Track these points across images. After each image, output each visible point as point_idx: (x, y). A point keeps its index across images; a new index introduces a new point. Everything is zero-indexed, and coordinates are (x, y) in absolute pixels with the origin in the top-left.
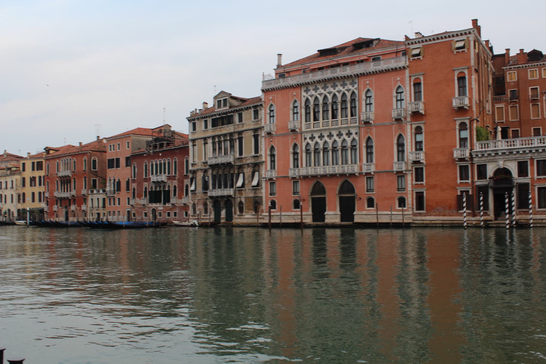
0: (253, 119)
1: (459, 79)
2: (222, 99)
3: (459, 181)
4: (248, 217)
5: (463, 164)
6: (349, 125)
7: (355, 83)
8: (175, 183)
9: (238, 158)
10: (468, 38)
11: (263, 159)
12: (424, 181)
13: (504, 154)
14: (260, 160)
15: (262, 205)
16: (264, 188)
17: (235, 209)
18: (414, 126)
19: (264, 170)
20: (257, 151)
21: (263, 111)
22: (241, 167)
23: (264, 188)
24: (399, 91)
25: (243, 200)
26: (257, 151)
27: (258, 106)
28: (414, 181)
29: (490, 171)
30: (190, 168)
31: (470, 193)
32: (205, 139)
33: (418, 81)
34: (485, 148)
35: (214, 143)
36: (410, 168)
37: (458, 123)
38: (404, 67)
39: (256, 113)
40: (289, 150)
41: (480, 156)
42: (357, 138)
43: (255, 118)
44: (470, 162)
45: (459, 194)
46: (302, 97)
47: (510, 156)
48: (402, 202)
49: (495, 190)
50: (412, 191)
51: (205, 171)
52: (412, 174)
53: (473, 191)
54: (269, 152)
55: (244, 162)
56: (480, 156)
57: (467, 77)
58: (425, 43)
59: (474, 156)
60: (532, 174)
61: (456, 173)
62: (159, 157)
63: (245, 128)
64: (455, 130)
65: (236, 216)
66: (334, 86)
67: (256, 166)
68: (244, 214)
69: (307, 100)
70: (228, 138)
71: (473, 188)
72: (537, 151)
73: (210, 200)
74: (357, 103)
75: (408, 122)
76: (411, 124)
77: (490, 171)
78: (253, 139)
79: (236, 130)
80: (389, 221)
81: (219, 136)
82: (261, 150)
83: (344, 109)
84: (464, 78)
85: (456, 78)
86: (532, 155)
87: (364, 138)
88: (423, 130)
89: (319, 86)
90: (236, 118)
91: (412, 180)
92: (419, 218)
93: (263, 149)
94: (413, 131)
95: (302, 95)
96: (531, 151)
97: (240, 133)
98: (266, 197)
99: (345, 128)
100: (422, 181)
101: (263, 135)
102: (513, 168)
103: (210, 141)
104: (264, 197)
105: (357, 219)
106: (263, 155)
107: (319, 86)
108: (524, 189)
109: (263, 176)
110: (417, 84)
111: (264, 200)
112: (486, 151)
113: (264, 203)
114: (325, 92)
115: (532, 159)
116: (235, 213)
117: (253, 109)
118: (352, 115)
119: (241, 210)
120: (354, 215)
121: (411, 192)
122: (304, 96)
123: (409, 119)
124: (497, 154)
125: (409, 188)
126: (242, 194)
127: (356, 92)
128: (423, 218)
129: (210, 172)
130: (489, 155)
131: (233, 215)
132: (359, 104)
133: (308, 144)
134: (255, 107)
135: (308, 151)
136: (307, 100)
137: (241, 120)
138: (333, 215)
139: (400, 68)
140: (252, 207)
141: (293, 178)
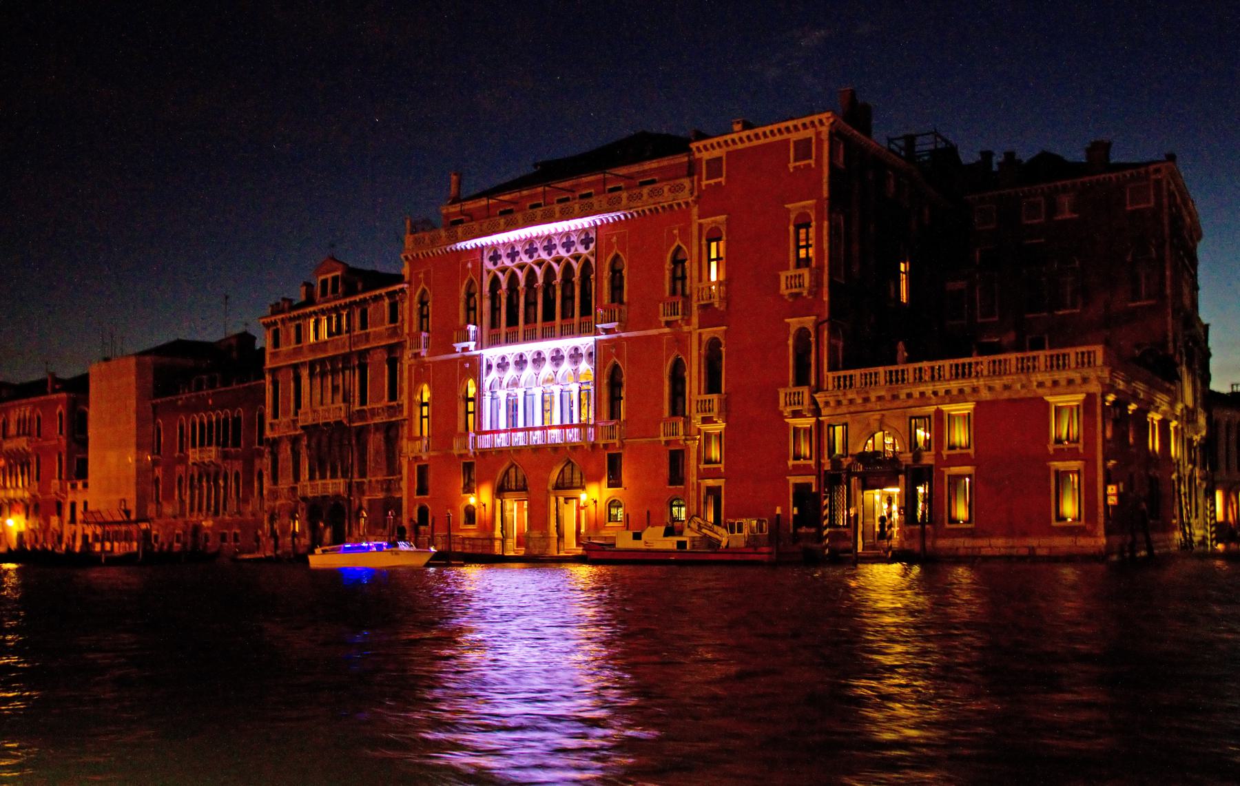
1: (798, 228)
8: (238, 466)
10: (818, 134)
20: (393, 395)
21: (406, 304)
24: (680, 257)
26: (393, 395)
30: (269, 434)
31: (814, 490)
32: (296, 367)
35: (312, 375)
39: (394, 308)
41: (832, 404)
47: (896, 404)
51: (295, 440)
53: (818, 486)
56: (832, 404)
58: (732, 148)
59: (821, 405)
62: (206, 409)
64: (787, 346)
71: (818, 478)
73: (303, 505)
81: (322, 362)
82: (401, 393)
83: (567, 299)
97: (363, 354)
103: (305, 373)
114: (530, 261)
117: (387, 301)
122: (489, 272)
125: (693, 479)
127: (592, 260)
129: (304, 442)
141: (461, 456)
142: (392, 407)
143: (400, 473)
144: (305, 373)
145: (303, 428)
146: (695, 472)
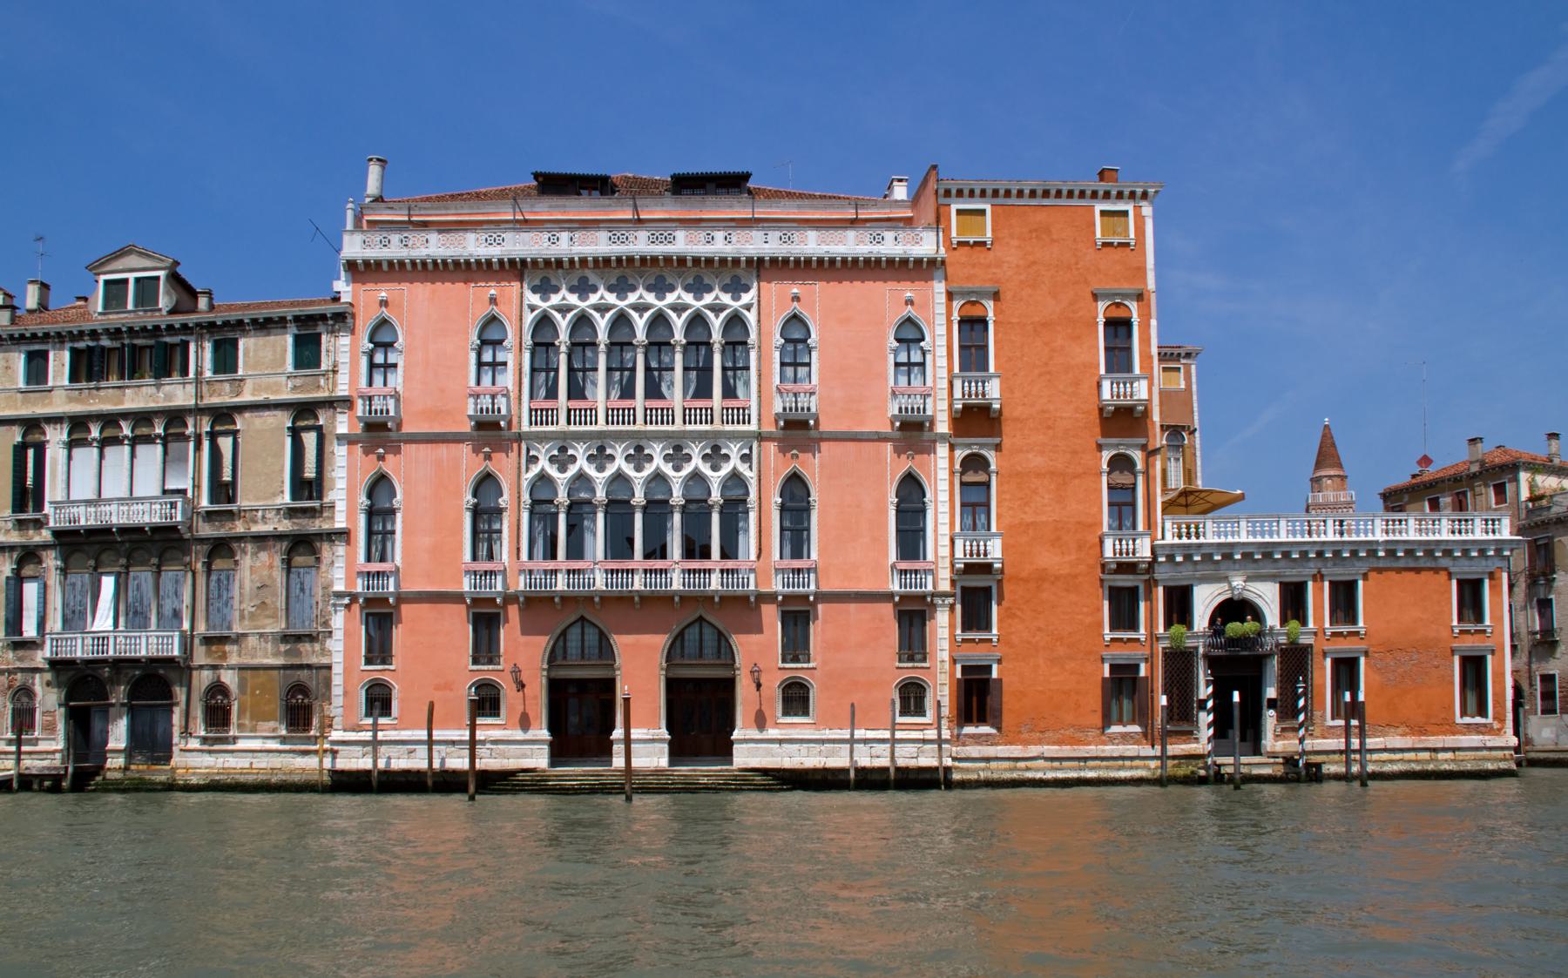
0: (290, 368)
1: (1109, 323)
2: (131, 276)
3: (1108, 634)
4: (257, 750)
6: (717, 426)
7: (747, 289)
9: (208, 513)
11: (340, 522)
12: (995, 631)
13: (1247, 556)
14: (317, 525)
15: (328, 698)
16: (339, 635)
17: (187, 714)
18: (960, 454)
19: (340, 564)
22: (222, 548)
23: (339, 635)
25: (229, 678)
27: (323, 317)
28: (959, 631)
29: (1205, 600)
35: (71, 445)
36: (945, 586)
37: (1106, 455)
40: (459, 496)
42: (750, 474)
43: (299, 364)
45: (1107, 674)
46: (525, 307)
48: (912, 697)
49: (1212, 662)
50: (954, 661)
52: (952, 607)
54: (363, 500)
55: (240, 528)
57: (1135, 319)
60: (1319, 619)
63: (247, 397)
65: (194, 744)
66: (736, 288)
67: (302, 547)
68: (233, 732)
69: (544, 322)
70: (159, 430)
72: (1337, 554)
74: (753, 355)
75: (943, 437)
76: (952, 448)
77: (1205, 600)
78: (288, 441)
79: (202, 403)
80: (884, 762)
84: (1127, 323)
85: (1101, 320)
86: (1319, 564)
87: (776, 474)
88: (993, 467)
89: (593, 279)
90: (202, 355)
91: (952, 626)
92: (974, 751)
93: (341, 484)
94: (957, 467)
95: (526, 302)
97: (223, 416)
98: (347, 671)
99: (700, 436)
100: (988, 628)
101: (342, 429)
102: (1267, 597)
103: (56, 437)
104: (338, 669)
105: (745, 756)
106: (341, 506)
107: (593, 279)
108: (1296, 659)
109: (339, 587)
110: (973, 325)
111: (337, 680)
112: (1200, 546)
113: (337, 690)
116: (187, 732)
118: (729, 392)
119: (218, 716)
120: (731, 743)
121: (947, 666)
122: (532, 308)
123: (943, 427)
124: (1228, 557)
126: (224, 656)
127: (751, 317)
128: (990, 751)
131: (176, 740)
132: (759, 358)
133: (543, 477)
134: (303, 321)
135: (541, 509)
136: (544, 322)
137: (226, 361)
138: (646, 746)
139: (918, 261)
140: (277, 706)
142: (304, 511)
143: (326, 624)
144: (56, 437)
145: (57, 533)
146: (946, 645)
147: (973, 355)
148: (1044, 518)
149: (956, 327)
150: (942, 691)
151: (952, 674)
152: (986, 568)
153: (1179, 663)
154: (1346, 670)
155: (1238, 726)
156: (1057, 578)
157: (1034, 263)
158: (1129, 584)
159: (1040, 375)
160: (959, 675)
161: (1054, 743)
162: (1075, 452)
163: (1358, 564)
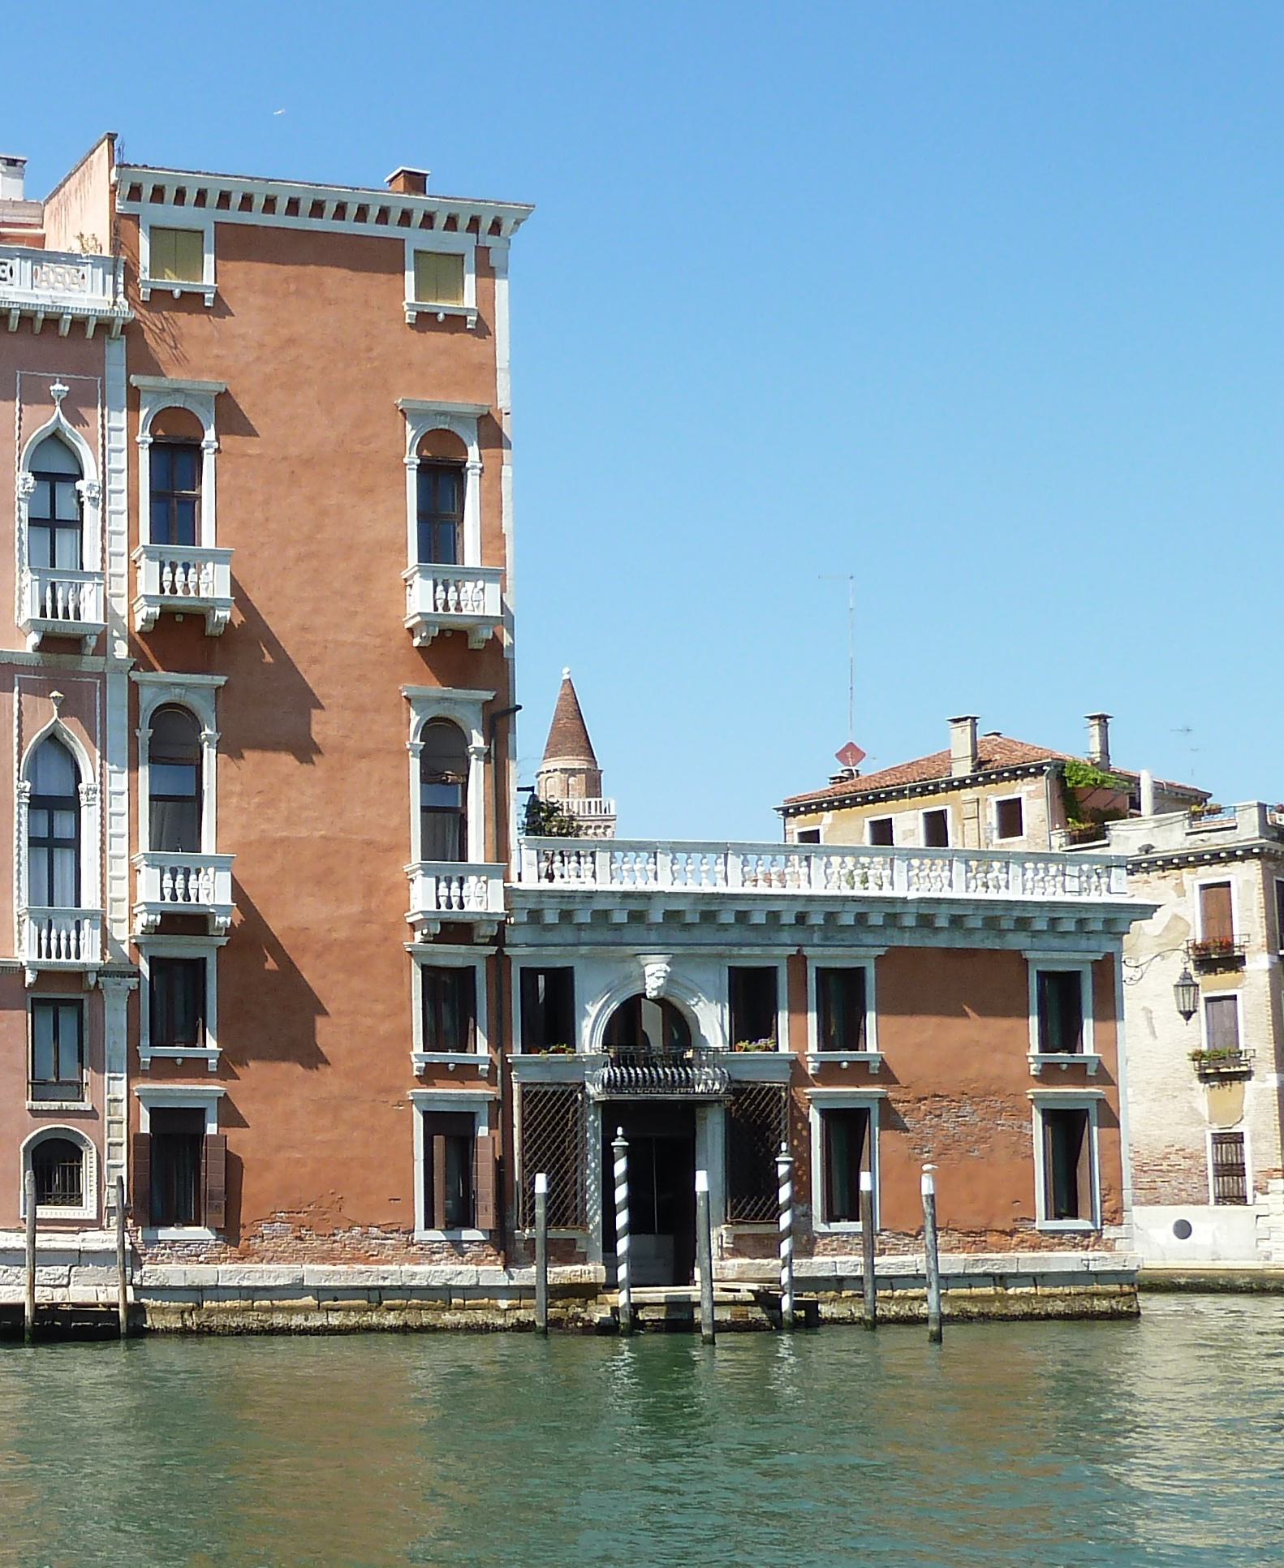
5: (453, 955)
18: (150, 700)
28: (145, 1040)
33: (184, 432)
34: (550, 877)
38: (104, 326)
44: (493, 950)
58: (233, 216)
61: (407, 1007)
76: (134, 686)
85: (412, 459)
86: (800, 937)
96: (801, 918)
115: (798, 962)
130: (602, 916)
139: (79, 323)
147: (173, 517)
148: (304, 833)
149: (144, 456)
150: (108, 1165)
151: (132, 1120)
152: (194, 923)
153: (551, 1117)
154: (848, 1128)
155: (666, 1230)
156: (328, 947)
157: (291, 341)
158: (458, 963)
159: (300, 558)
160: (145, 1128)
161: (323, 1260)
162: (360, 710)
163: (869, 939)
